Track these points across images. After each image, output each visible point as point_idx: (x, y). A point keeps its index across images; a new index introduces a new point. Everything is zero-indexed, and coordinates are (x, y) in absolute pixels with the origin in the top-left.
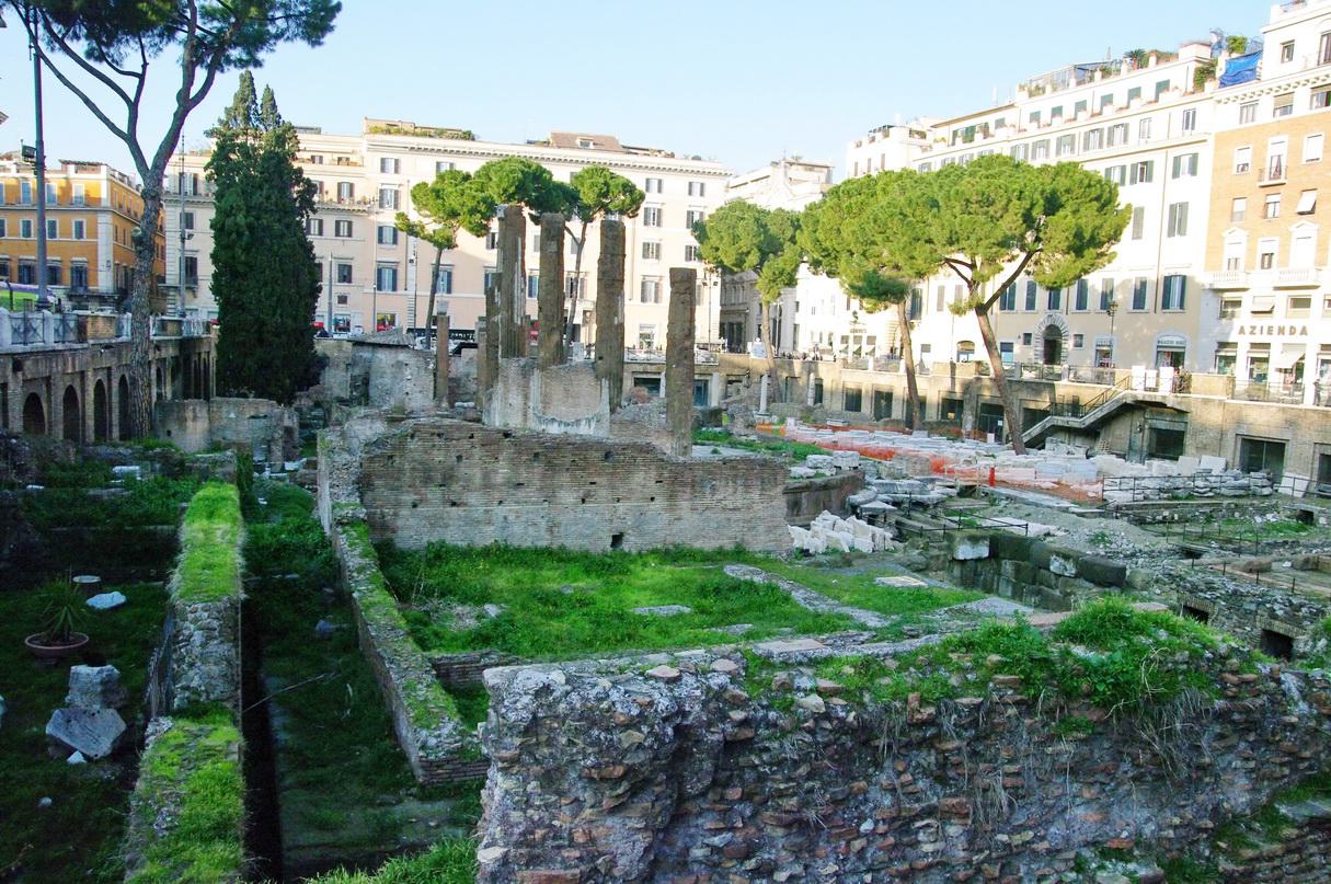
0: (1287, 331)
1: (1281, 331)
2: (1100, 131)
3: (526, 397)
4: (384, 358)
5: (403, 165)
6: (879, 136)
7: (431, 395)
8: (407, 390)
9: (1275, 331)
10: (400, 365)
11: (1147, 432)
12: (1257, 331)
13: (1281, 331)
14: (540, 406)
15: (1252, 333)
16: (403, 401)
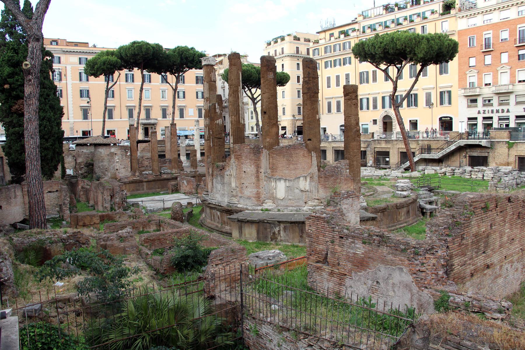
0: (500, 111)
1: (498, 111)
4: (102, 151)
5: (62, 60)
6: (279, 40)
7: (130, 169)
8: (117, 167)
9: (495, 111)
10: (113, 155)
11: (468, 158)
12: (486, 112)
13: (498, 111)
14: (269, 171)
15: (484, 113)
16: (115, 174)
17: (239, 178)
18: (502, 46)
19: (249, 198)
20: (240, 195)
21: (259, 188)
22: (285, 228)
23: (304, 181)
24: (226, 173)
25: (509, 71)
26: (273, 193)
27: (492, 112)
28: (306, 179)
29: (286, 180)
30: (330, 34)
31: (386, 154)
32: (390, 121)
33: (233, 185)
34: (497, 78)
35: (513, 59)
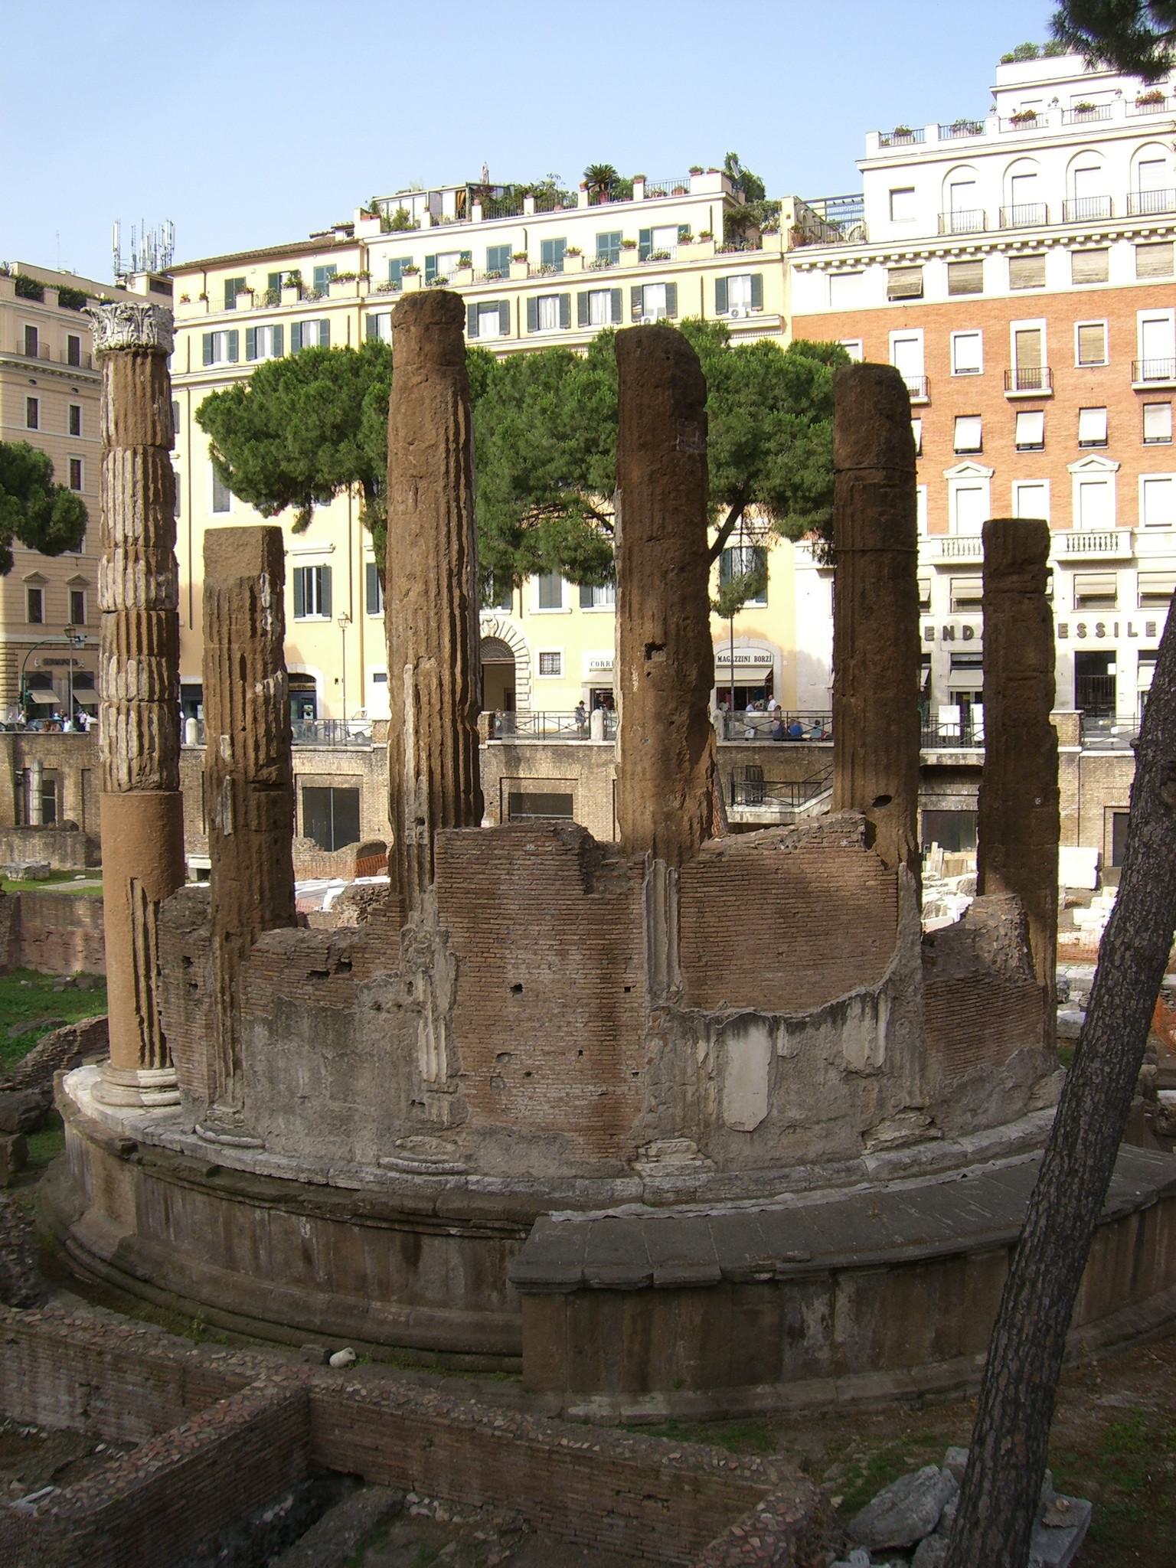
0: (959, 634)
2: (564, 300)
3: (610, 957)
18: (958, 392)
19: (548, 1136)
21: (617, 1078)
22: (859, 1301)
23: (868, 1022)
24: (367, 998)
25: (985, 483)
26: (701, 1100)
28: (875, 1009)
29: (773, 1026)
30: (229, 284)
32: (503, 660)
33: (432, 1062)
34: (945, 508)
35: (1003, 442)
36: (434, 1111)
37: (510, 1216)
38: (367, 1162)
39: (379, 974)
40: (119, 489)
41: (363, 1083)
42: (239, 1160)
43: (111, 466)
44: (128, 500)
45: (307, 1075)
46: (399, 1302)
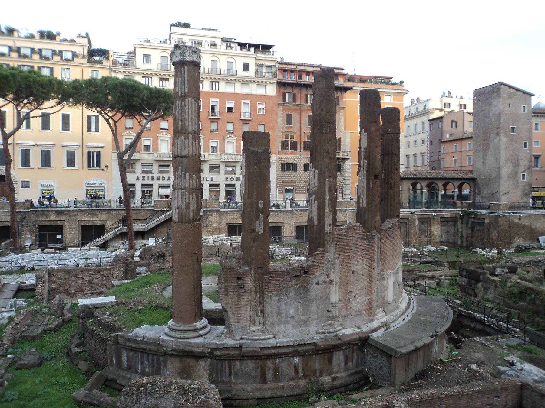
0: (161, 179)
1: (158, 179)
9: (155, 178)
12: (146, 178)
13: (158, 179)
15: (143, 180)
17: (343, 284)
20: (344, 313)
24: (315, 281)
27: (153, 179)
31: (59, 229)
33: (335, 298)
34: (158, 144)
36: (334, 312)
37: (360, 339)
38: (313, 333)
39: (318, 273)
40: (190, 113)
41: (313, 308)
42: (271, 344)
43: (187, 104)
44: (193, 117)
45: (293, 309)
46: (326, 375)
